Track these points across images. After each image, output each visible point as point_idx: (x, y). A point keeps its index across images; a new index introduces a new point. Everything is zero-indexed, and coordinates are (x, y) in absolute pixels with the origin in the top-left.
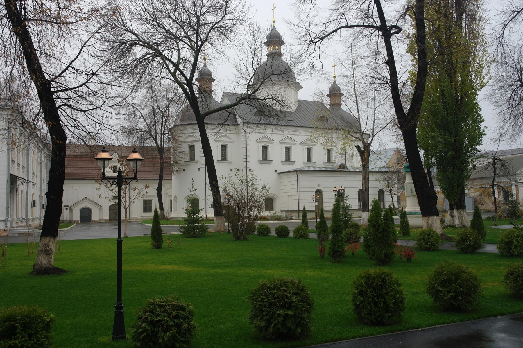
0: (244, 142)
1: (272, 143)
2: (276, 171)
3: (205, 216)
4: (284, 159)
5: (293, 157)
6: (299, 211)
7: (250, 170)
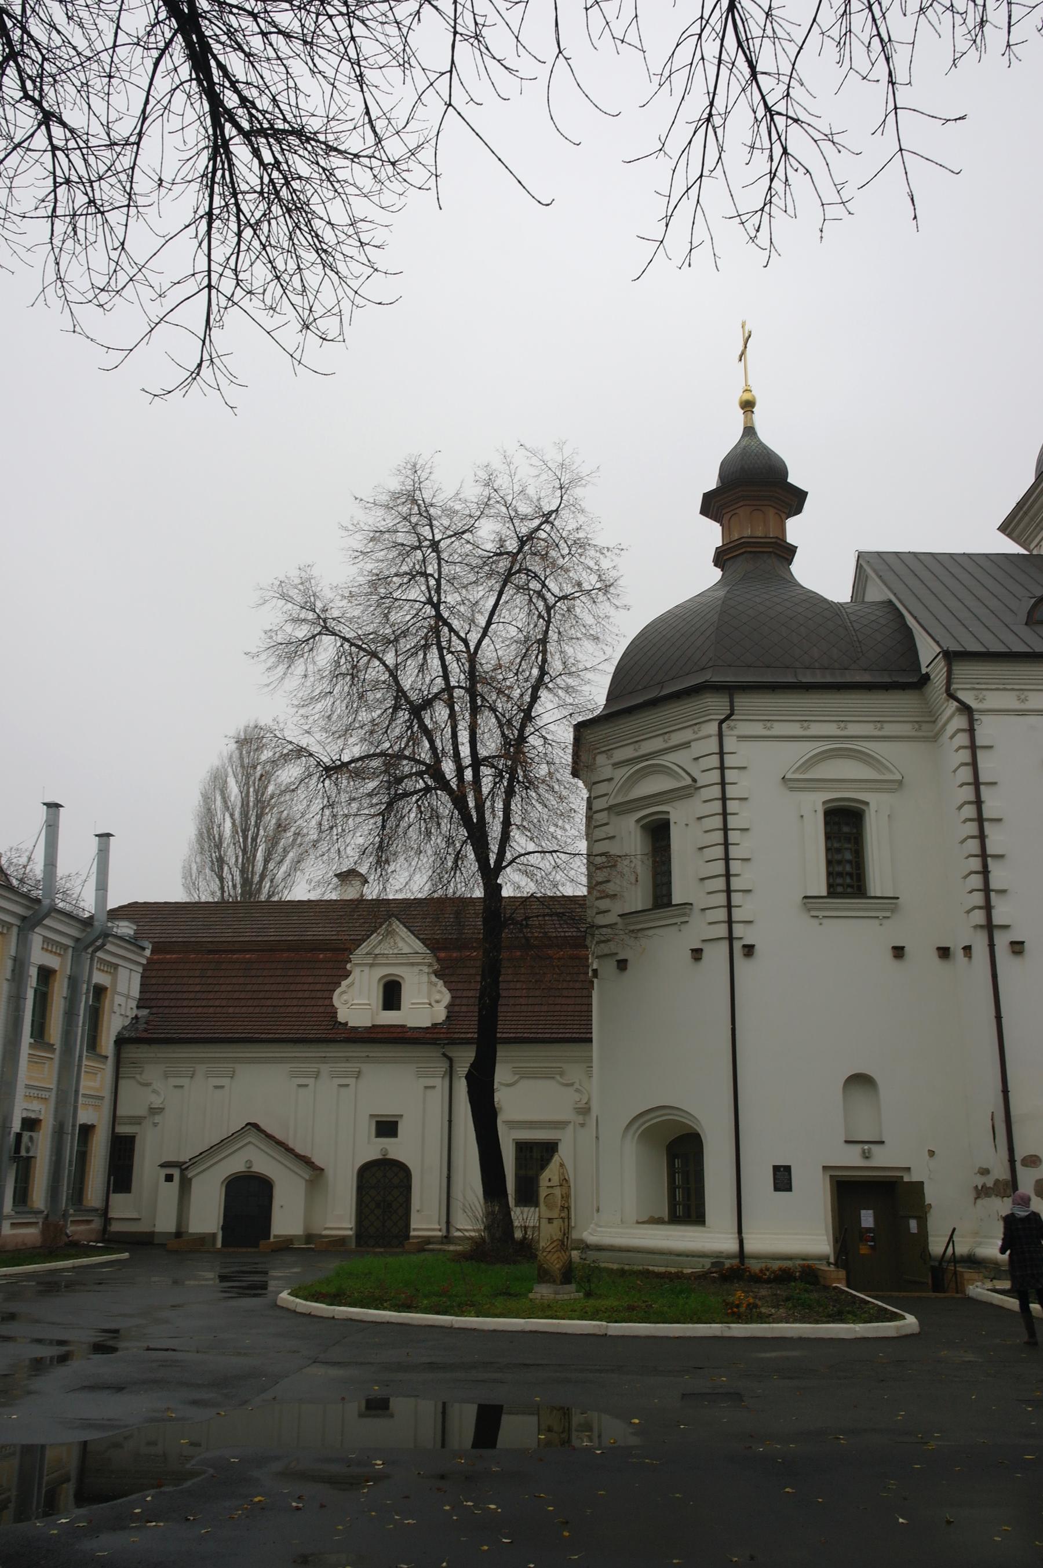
0: (966, 775)
3: (730, 1245)
7: (1017, 948)
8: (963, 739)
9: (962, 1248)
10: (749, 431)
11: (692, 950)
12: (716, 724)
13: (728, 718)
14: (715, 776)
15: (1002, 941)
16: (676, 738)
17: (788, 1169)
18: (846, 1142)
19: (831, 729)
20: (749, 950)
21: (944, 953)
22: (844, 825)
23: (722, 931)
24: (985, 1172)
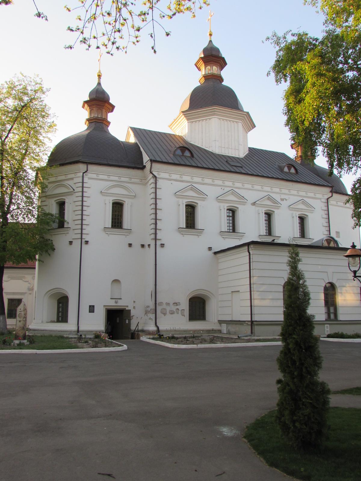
1: (203, 199)
2: (210, 249)
4: (225, 228)
5: (241, 226)
6: (252, 322)
7: (162, 245)
8: (153, 185)
9: (140, 328)
10: (99, 84)
11: (69, 242)
12: (82, 173)
13: (86, 172)
14: (80, 189)
15: (159, 243)
16: (70, 176)
17: (93, 306)
18: (111, 299)
19: (116, 178)
20: (87, 242)
21: (143, 246)
22: (118, 208)
23: (79, 236)
24: (148, 307)
